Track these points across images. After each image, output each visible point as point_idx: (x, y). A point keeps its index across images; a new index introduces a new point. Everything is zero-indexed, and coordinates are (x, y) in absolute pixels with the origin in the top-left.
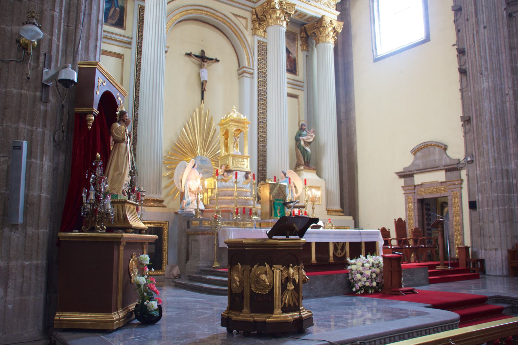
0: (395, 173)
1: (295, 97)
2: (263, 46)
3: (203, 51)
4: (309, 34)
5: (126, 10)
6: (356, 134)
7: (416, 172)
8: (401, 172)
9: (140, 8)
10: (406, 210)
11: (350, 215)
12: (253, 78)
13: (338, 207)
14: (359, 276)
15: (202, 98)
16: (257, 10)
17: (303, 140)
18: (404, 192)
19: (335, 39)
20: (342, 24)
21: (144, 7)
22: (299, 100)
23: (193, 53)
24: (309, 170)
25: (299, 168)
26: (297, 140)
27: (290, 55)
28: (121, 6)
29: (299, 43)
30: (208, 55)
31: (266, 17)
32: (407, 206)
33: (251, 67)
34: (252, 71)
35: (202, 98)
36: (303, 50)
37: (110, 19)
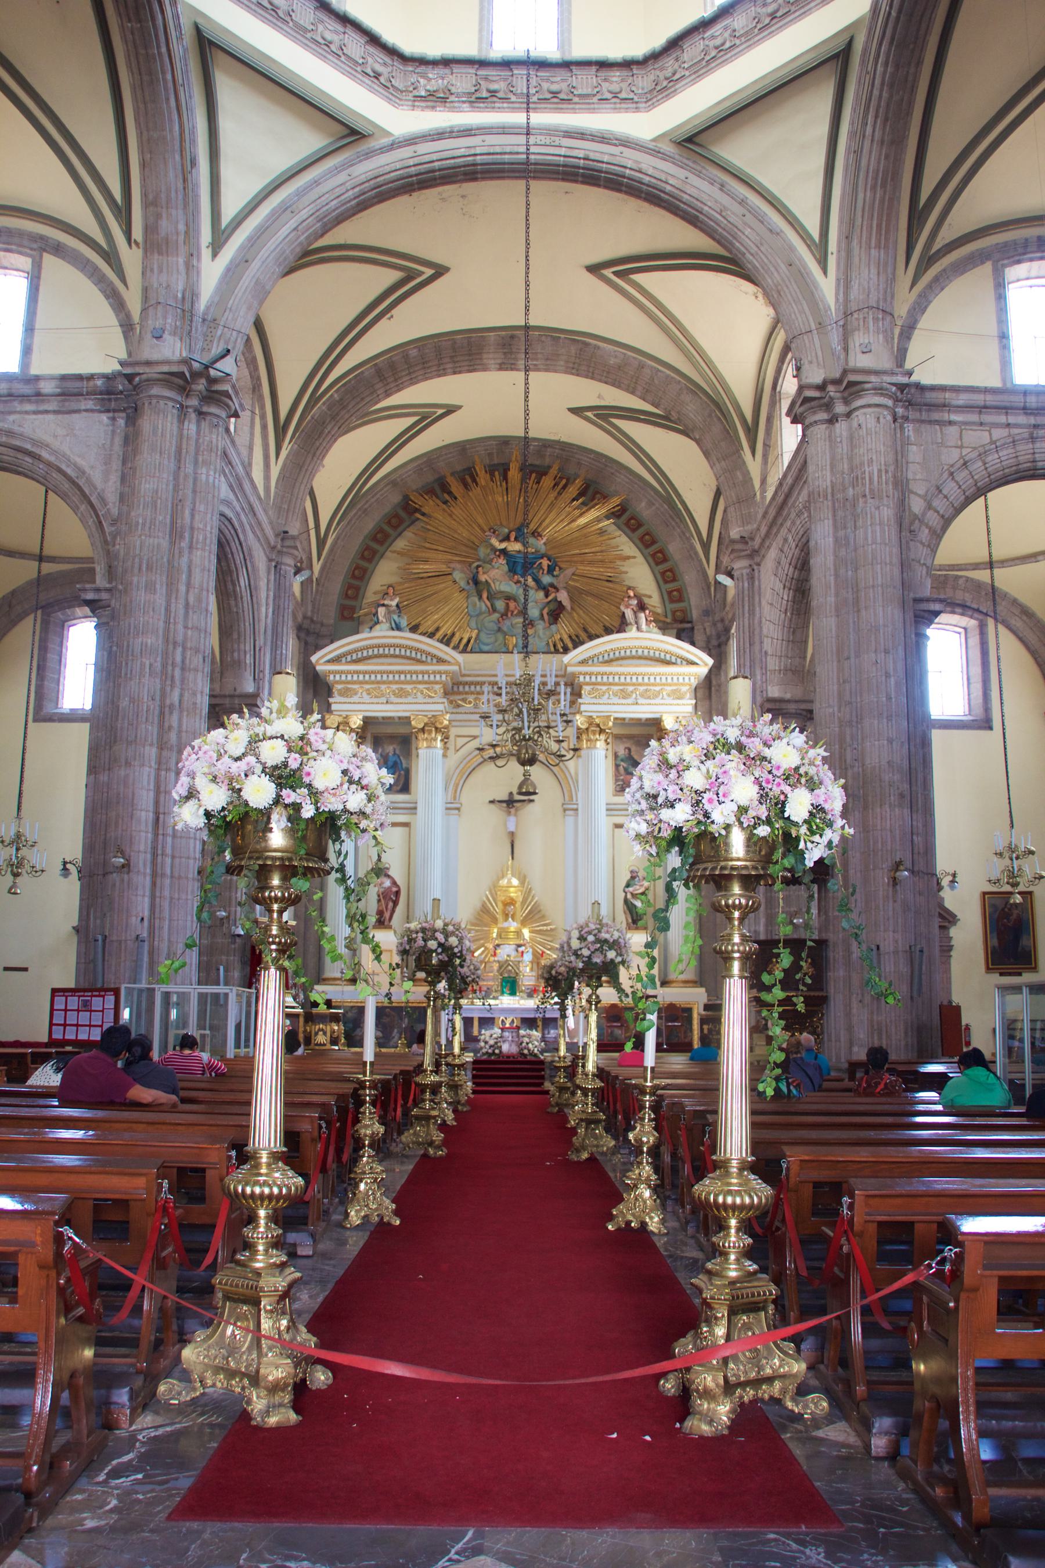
11: (702, 986)
23: (497, 799)
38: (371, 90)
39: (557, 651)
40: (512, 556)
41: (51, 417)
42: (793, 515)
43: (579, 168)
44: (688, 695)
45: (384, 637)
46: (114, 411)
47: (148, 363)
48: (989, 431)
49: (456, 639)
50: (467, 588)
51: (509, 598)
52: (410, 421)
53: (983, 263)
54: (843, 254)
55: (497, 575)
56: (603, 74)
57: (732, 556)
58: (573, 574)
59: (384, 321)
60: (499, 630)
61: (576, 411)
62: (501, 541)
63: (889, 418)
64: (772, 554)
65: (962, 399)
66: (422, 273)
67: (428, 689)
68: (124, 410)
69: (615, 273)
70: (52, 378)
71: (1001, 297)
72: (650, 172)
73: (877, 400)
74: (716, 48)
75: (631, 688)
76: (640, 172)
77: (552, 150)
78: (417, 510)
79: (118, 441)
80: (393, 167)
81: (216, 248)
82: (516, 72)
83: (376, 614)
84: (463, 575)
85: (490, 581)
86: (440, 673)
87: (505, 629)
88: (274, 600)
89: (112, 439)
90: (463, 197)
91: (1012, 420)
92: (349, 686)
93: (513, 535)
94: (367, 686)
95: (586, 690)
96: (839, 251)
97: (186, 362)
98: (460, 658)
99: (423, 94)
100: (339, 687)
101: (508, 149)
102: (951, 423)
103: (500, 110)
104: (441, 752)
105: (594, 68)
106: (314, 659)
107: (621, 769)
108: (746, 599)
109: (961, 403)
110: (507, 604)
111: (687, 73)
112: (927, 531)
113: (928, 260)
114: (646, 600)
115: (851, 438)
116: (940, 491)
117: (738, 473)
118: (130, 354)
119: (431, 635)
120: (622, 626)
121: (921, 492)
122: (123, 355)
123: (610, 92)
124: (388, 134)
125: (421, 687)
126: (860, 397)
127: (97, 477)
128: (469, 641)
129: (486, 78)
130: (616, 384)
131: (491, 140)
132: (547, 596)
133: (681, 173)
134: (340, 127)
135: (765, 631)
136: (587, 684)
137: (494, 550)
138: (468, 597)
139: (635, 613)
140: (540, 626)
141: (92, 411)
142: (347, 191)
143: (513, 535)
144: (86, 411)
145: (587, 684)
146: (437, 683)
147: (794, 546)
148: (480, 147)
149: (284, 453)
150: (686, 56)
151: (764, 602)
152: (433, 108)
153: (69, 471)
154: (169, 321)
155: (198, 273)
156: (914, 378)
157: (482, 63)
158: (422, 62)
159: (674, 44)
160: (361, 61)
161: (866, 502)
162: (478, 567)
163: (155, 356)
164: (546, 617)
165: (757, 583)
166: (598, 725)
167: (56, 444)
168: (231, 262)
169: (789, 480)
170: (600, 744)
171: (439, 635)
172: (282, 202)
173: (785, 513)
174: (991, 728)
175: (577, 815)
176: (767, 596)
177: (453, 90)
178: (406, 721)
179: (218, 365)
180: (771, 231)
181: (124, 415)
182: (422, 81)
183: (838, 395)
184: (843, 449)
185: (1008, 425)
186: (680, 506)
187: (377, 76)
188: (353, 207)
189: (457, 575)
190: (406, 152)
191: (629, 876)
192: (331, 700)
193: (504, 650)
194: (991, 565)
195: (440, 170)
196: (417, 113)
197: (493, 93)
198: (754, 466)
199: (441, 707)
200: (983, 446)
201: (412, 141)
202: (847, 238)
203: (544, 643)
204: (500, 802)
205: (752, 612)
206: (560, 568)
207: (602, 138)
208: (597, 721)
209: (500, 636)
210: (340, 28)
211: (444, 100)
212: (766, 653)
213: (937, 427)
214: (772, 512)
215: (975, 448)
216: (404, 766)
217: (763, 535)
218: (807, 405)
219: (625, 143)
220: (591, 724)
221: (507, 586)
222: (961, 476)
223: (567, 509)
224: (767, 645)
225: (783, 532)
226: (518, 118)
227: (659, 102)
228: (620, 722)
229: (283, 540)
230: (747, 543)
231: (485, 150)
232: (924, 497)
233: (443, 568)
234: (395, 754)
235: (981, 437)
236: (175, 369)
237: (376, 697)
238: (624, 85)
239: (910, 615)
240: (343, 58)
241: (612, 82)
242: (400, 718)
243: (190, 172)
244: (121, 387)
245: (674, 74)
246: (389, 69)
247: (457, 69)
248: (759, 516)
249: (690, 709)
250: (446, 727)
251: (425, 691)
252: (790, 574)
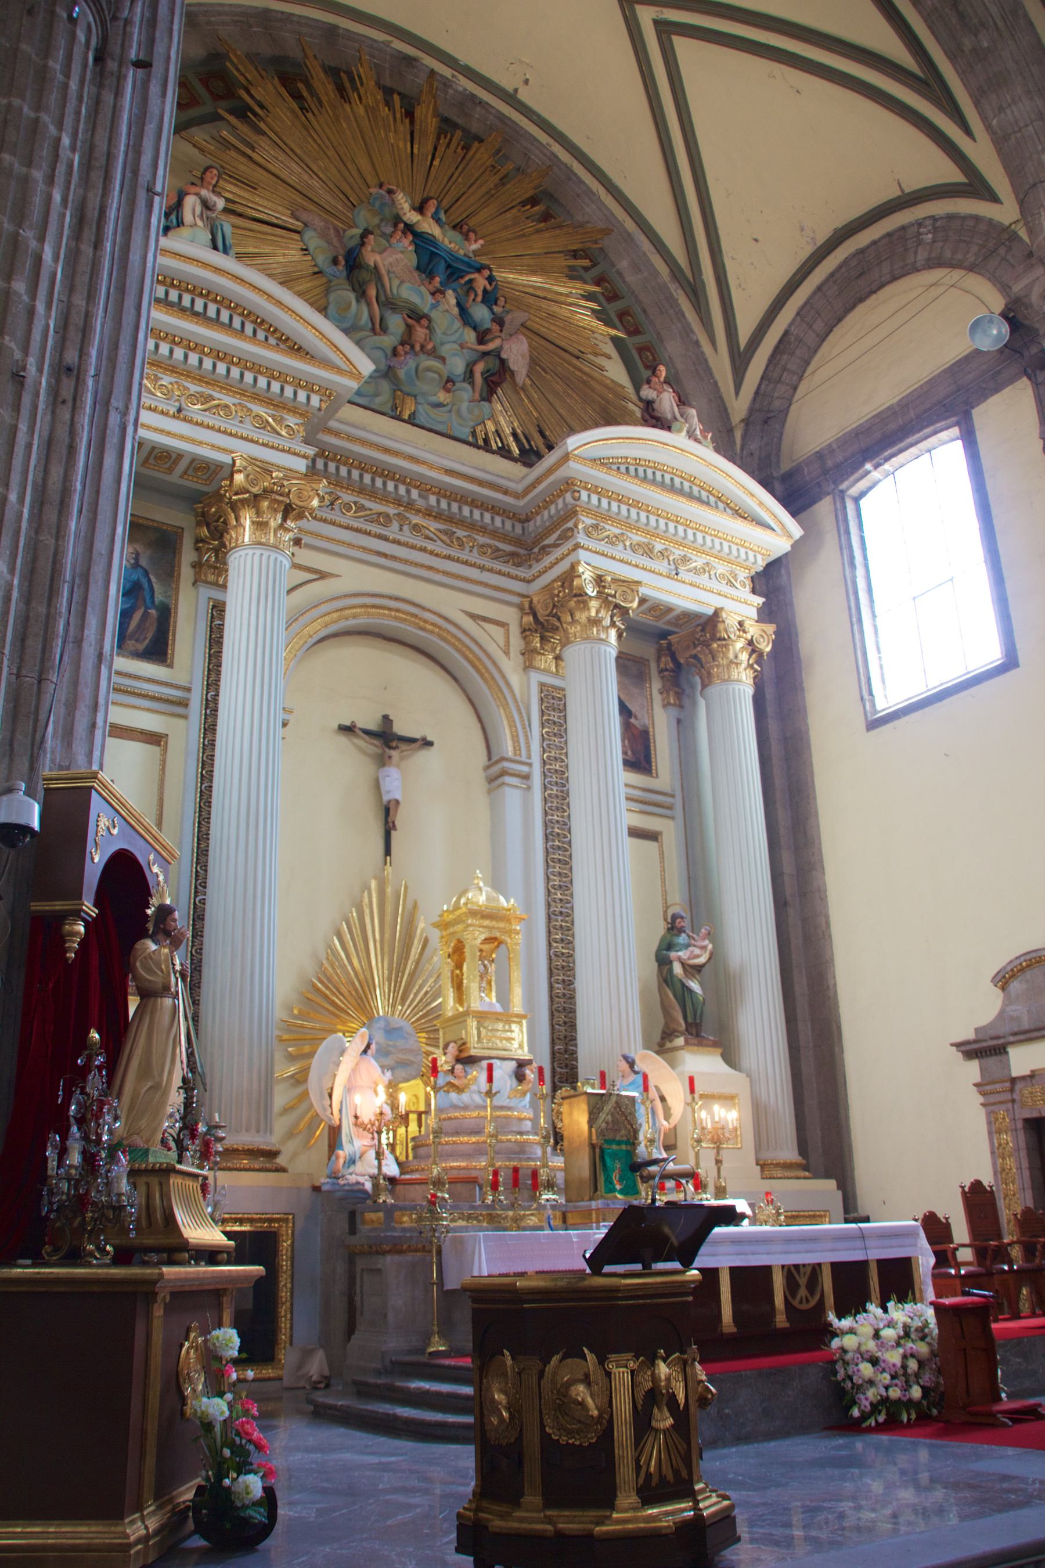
0: (952, 1045)
1: (652, 836)
2: (553, 698)
3: (386, 718)
4: (682, 661)
5: (176, 613)
6: (830, 936)
7: (1012, 1039)
8: (967, 1043)
9: (214, 607)
10: (992, 1153)
11: (827, 1176)
12: (529, 788)
13: (790, 1153)
14: (866, 1369)
15: (388, 851)
16: (535, 600)
17: (680, 959)
18: (981, 1099)
19: (756, 671)
20: (771, 629)
21: (224, 603)
22: (661, 847)
23: (361, 724)
24: (701, 1048)
25: (671, 1041)
26: (663, 961)
27: (633, 720)
28: (162, 603)
29: (656, 685)
30: (400, 728)
31: (559, 619)
32: (995, 1141)
33: (524, 759)
34: (525, 769)
35: (388, 851)
36: (666, 705)
37: (130, 639)
51: (416, 316)
84: (323, 244)
85: (383, 272)
87: (401, 373)
95: (586, 521)
132: (481, 341)
136: (589, 512)
137: (397, 219)
138: (327, 292)
140: (465, 394)
164: (478, 379)
203: (468, 430)
216: (159, 597)
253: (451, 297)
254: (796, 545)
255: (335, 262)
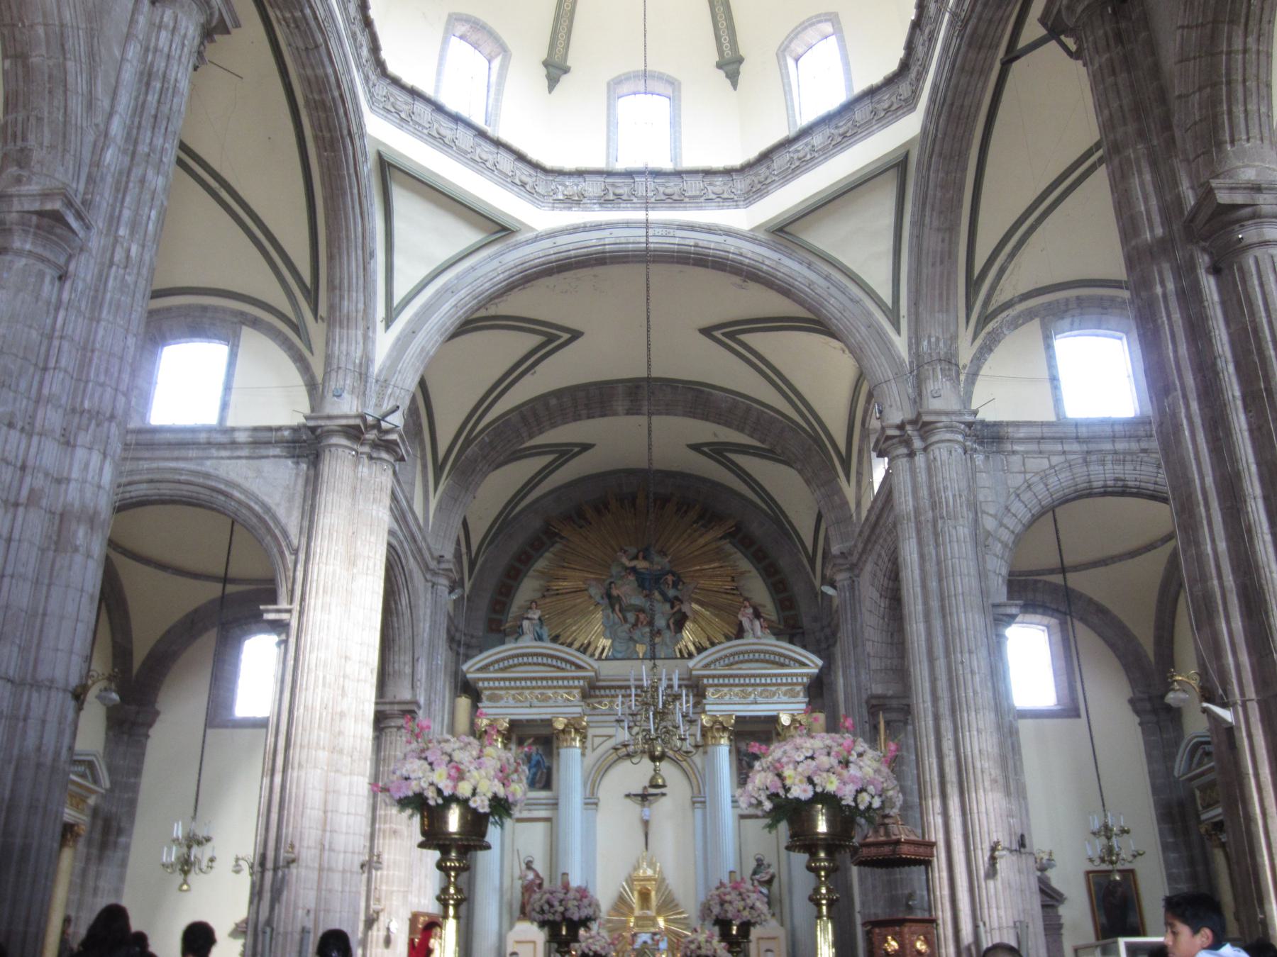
38: (518, 195)
39: (682, 657)
40: (642, 573)
41: (244, 461)
42: (884, 534)
43: (690, 253)
44: (802, 694)
45: (527, 647)
46: (298, 457)
47: (330, 417)
48: (1048, 458)
49: (591, 649)
50: (601, 601)
52: (548, 459)
53: (1032, 319)
54: (913, 317)
55: (628, 591)
56: (708, 179)
57: (834, 570)
58: (695, 588)
59: (528, 377)
60: (631, 639)
61: (696, 448)
62: (631, 560)
63: (960, 451)
64: (869, 567)
65: (1022, 433)
66: (559, 337)
67: (568, 694)
68: (307, 456)
69: (724, 334)
70: (246, 429)
71: (1049, 347)
72: (750, 255)
73: (949, 436)
74: (799, 159)
75: (750, 689)
76: (741, 255)
77: (668, 240)
78: (556, 534)
79: (301, 482)
80: (536, 255)
81: (389, 321)
82: (637, 179)
83: (521, 626)
86: (578, 678)
87: (636, 638)
88: (431, 616)
89: (296, 480)
90: (595, 276)
91: (1067, 448)
92: (497, 692)
93: (641, 555)
94: (513, 692)
96: (909, 315)
97: (363, 417)
98: (596, 665)
99: (561, 197)
100: (487, 692)
101: (631, 240)
102: (1014, 452)
103: (626, 209)
104: (579, 751)
105: (701, 175)
106: (465, 667)
107: (744, 763)
108: (848, 607)
109: (1021, 435)
110: (638, 617)
111: (777, 178)
112: (1000, 545)
113: (985, 319)
114: (761, 610)
115: (929, 469)
116: (1009, 510)
117: (836, 498)
118: (313, 410)
119: (570, 645)
120: (740, 633)
121: (992, 511)
122: (306, 409)
123: (714, 193)
124: (532, 229)
125: (561, 691)
126: (934, 434)
127: (281, 513)
128: (603, 649)
129: (613, 185)
130: (728, 424)
131: (617, 232)
132: (672, 607)
133: (775, 256)
134: (491, 224)
135: (866, 635)
136: (711, 686)
137: (626, 568)
139: (751, 621)
140: (668, 635)
141: (279, 457)
142: (499, 275)
143: (641, 555)
144: (275, 456)
145: (711, 686)
146: (575, 687)
147: (886, 560)
148: (608, 240)
149: (441, 488)
150: (775, 165)
151: (864, 610)
152: (570, 208)
153: (257, 508)
154: (348, 382)
155: (374, 342)
156: (979, 417)
157: (609, 174)
158: (560, 173)
159: (766, 156)
160: (510, 174)
161: (944, 523)
162: (611, 583)
163: (335, 412)
164: (672, 626)
165: (857, 593)
166: (721, 723)
167: (247, 485)
168: (401, 333)
169: (879, 504)
170: (725, 741)
171: (577, 645)
172: (445, 284)
173: (877, 531)
174: (1078, 716)
175: (705, 808)
176: (867, 604)
177: (586, 194)
178: (548, 723)
179: (388, 419)
180: (851, 300)
181: (306, 460)
182: (560, 187)
183: (915, 433)
184: (922, 477)
185: (1064, 453)
186: (787, 526)
187: (524, 185)
188: (502, 288)
189: (593, 591)
190: (547, 243)
191: (753, 864)
192: (480, 705)
193: (635, 656)
194: (1063, 570)
195: (575, 257)
196: (557, 212)
197: (618, 196)
198: (849, 491)
199: (579, 710)
200: (1044, 471)
201: (552, 234)
202: (915, 303)
204: (635, 795)
205: (854, 618)
206: (684, 583)
207: (710, 230)
208: (720, 719)
209: (631, 644)
210: (494, 149)
211: (578, 202)
212: (868, 654)
213: (1003, 457)
214: (867, 532)
215: (1037, 473)
217: (860, 550)
218: (890, 442)
219: (729, 233)
220: (715, 723)
221: (637, 600)
222: (1026, 496)
223: (689, 531)
224: (869, 648)
225: (878, 547)
226: (640, 215)
227: (755, 201)
228: (740, 720)
229: (439, 562)
230: (846, 558)
231: (612, 241)
232: (995, 516)
233: (581, 585)
234: (537, 754)
235: (1040, 464)
236: (352, 422)
237: (521, 701)
238: (726, 188)
239: (990, 619)
240: (496, 172)
241: (715, 186)
242: (542, 720)
243: (369, 263)
244: (304, 437)
245: (766, 179)
246: (534, 179)
247: (588, 178)
248: (856, 534)
249: (803, 706)
250: (584, 728)
251: (565, 695)
252: (885, 584)
253: (657, 595)
254: (821, 670)
255: (602, 598)
